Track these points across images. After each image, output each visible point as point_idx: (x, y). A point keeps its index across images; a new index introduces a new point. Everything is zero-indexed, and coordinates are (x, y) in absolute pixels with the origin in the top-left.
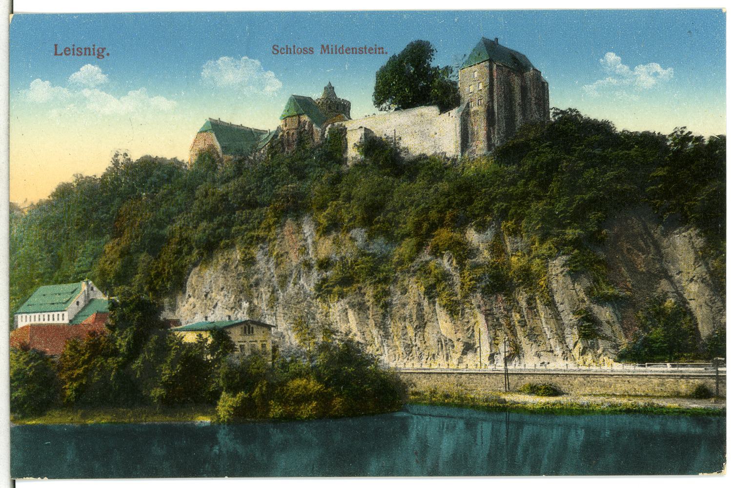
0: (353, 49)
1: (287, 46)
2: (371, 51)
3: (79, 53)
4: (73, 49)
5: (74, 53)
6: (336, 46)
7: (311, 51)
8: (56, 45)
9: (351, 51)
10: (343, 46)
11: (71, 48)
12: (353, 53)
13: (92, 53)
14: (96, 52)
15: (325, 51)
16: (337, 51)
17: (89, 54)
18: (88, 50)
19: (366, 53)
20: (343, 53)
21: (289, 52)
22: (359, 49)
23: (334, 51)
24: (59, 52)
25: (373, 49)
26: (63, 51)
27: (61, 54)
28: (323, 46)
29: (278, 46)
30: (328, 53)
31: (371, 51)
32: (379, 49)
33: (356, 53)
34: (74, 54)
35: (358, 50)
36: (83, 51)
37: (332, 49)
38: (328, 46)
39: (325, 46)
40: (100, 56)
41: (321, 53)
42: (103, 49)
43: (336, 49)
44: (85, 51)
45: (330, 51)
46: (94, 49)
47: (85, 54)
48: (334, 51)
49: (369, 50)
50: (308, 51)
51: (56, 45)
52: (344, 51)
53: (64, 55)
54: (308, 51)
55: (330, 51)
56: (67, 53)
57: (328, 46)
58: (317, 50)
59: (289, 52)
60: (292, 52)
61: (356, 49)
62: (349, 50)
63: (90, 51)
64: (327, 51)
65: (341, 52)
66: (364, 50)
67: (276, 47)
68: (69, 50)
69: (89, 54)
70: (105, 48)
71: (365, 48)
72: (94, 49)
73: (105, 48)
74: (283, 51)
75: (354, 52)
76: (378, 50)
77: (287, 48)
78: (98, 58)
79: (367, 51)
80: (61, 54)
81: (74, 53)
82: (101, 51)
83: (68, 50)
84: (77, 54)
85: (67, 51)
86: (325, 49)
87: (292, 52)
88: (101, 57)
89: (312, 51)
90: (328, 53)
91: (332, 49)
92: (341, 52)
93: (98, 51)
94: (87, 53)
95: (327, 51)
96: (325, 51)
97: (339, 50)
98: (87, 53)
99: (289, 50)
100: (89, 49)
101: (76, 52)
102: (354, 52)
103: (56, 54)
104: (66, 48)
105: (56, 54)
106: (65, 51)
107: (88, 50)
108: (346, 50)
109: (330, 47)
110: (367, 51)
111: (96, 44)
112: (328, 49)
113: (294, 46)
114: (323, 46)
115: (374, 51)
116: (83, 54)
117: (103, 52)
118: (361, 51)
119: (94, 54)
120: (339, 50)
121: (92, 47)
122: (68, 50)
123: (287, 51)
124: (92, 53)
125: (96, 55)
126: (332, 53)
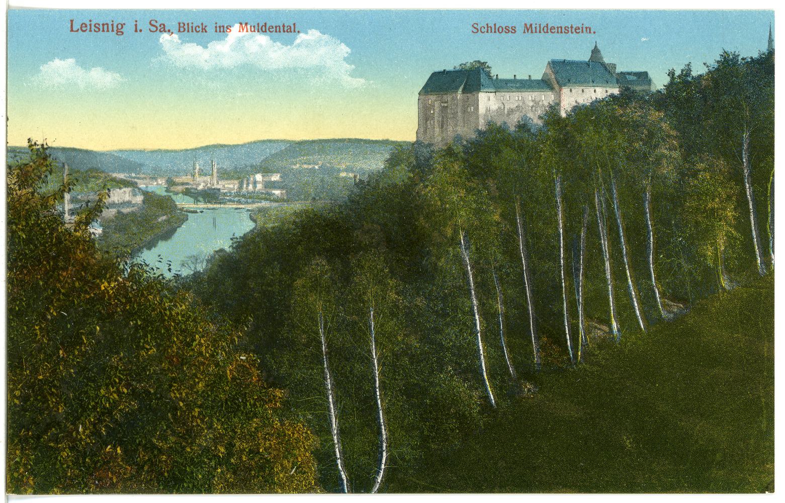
0: (558, 28)
2: (578, 31)
6: (540, 25)
7: (514, 30)
15: (528, 31)
16: (542, 30)
19: (572, 33)
20: (547, 32)
21: (489, 31)
22: (95, 26)
25: (579, 29)
28: (526, 25)
30: (532, 32)
31: (578, 31)
33: (561, 32)
35: (563, 30)
37: (536, 28)
38: (531, 25)
39: (528, 26)
41: (524, 32)
44: (103, 28)
45: (534, 30)
47: (103, 31)
49: (576, 29)
50: (510, 29)
52: (549, 31)
54: (510, 29)
55: (534, 30)
57: (531, 25)
58: (520, 29)
59: (489, 31)
60: (493, 31)
61: (561, 27)
64: (530, 31)
65: (545, 30)
66: (570, 30)
71: (572, 27)
76: (584, 30)
77: (488, 27)
79: (573, 30)
86: (528, 28)
87: (493, 31)
89: (514, 30)
90: (532, 32)
91: (536, 28)
92: (545, 29)
95: (530, 31)
96: (528, 31)
97: (543, 29)
108: (551, 29)
109: (533, 26)
110: (573, 30)
111: (194, 23)
112: (532, 29)
114: (526, 25)
115: (581, 30)
120: (543, 29)
123: (488, 30)
126: (536, 32)
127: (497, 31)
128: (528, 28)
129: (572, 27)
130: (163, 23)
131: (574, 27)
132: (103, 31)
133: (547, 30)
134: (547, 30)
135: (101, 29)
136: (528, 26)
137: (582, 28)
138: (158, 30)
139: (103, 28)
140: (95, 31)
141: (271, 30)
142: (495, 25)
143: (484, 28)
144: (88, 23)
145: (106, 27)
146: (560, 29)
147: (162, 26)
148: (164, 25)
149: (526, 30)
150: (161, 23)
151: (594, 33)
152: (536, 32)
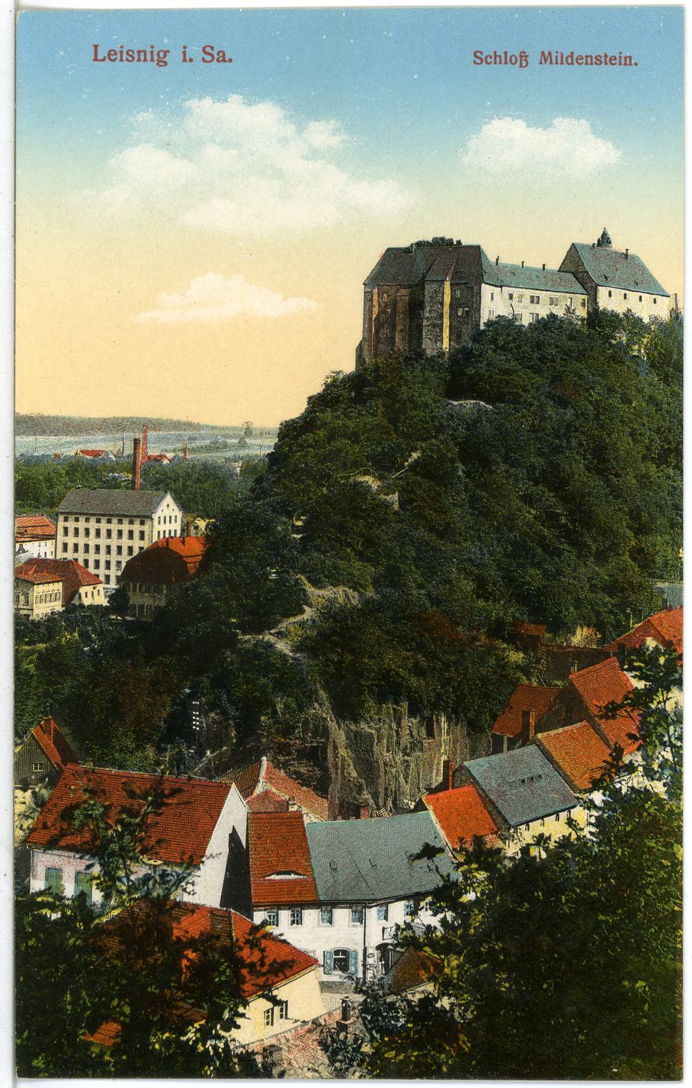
0: (587, 57)
1: (495, 53)
2: (614, 62)
3: (130, 59)
4: (121, 52)
5: (122, 56)
8: (96, 47)
9: (584, 61)
10: (572, 53)
12: (587, 64)
13: (149, 57)
14: (155, 57)
15: (546, 60)
17: (145, 60)
18: (142, 54)
19: (606, 64)
20: (572, 63)
23: (559, 61)
24: (100, 57)
25: (616, 59)
26: (106, 55)
27: (104, 60)
28: (543, 53)
29: (481, 53)
30: (551, 63)
31: (614, 62)
32: (625, 58)
33: (592, 64)
34: (121, 60)
35: (594, 60)
36: (136, 56)
37: (557, 57)
39: (546, 54)
40: (162, 62)
41: (541, 63)
42: (166, 53)
43: (562, 58)
44: (139, 55)
45: (554, 61)
46: (152, 52)
48: (559, 61)
49: (610, 60)
51: (96, 47)
52: (574, 62)
53: (107, 60)
55: (554, 61)
56: (113, 57)
57: (550, 54)
58: (534, 58)
60: (503, 61)
62: (582, 59)
63: (145, 55)
65: (570, 61)
66: (603, 60)
67: (478, 54)
68: (116, 54)
69: (145, 60)
70: (168, 51)
71: (606, 56)
72: (152, 52)
73: (168, 51)
74: (489, 60)
75: (589, 62)
76: (623, 60)
78: (158, 64)
79: (608, 60)
80: (104, 60)
81: (122, 56)
82: (162, 55)
83: (112, 53)
84: (127, 60)
85: (111, 56)
86: (546, 58)
87: (503, 61)
88: (161, 64)
90: (551, 63)
91: (557, 57)
92: (570, 61)
93: (158, 54)
94: (142, 58)
96: (546, 60)
98: (142, 58)
99: (498, 59)
100: (145, 52)
101: (125, 56)
102: (589, 62)
103: (96, 59)
104: (111, 51)
105: (96, 59)
106: (109, 54)
107: (142, 54)
108: (577, 59)
109: (554, 55)
110: (608, 60)
112: (551, 58)
113: (506, 53)
114: (543, 53)
115: (618, 61)
117: (165, 56)
118: (598, 60)
119: (152, 60)
120: (567, 63)
121: (149, 50)
122: (112, 53)
124: (149, 57)
125: (156, 62)
126: (557, 63)
127: (508, 61)
128: (546, 58)
129: (606, 56)
131: (609, 55)
132: (139, 60)
133: (572, 59)
134: (572, 59)
135: (603, 61)
136: (546, 54)
137: (620, 58)
141: (580, 61)
142: (506, 53)
143: (491, 58)
144: (617, 56)
145: (589, 59)
146: (589, 59)
149: (543, 61)
151: (636, 64)
152: (557, 63)
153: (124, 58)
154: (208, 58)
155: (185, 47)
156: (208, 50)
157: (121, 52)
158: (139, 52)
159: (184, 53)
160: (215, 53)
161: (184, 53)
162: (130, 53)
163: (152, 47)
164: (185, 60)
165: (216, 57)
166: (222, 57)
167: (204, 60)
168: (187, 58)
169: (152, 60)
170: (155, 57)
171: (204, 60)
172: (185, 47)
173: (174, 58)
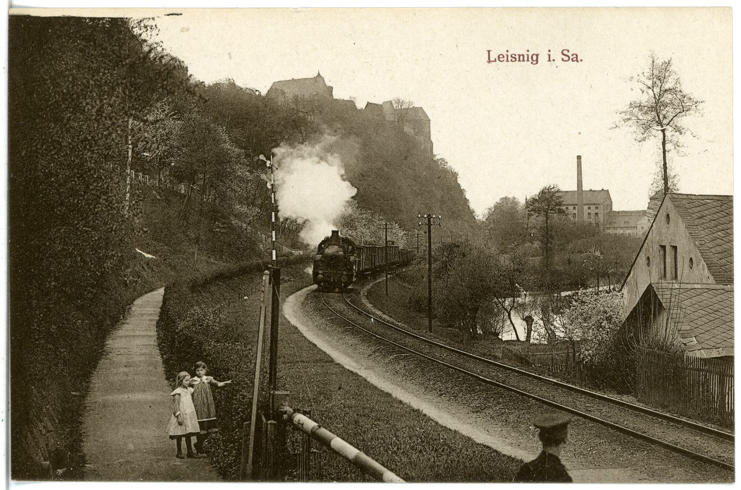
3: (514, 60)
5: (507, 59)
11: (505, 54)
13: (526, 58)
14: (530, 59)
17: (524, 60)
36: (517, 57)
44: (519, 58)
47: (519, 61)
68: (504, 57)
78: (532, 63)
80: (495, 61)
81: (507, 59)
101: (510, 58)
104: (501, 55)
106: (499, 57)
116: (518, 59)
119: (528, 60)
124: (526, 58)
130: (576, 53)
132: (519, 61)
138: (571, 59)
139: (519, 58)
140: (511, 60)
147: (575, 56)
148: (577, 55)
150: (512, 53)
153: (509, 60)
154: (566, 58)
155: (549, 51)
156: (565, 52)
157: (507, 55)
158: (519, 56)
159: (549, 55)
160: (570, 54)
161: (549, 55)
162: (513, 56)
163: (528, 51)
164: (549, 60)
165: (571, 57)
166: (576, 58)
167: (563, 60)
168: (551, 59)
169: (528, 60)
170: (530, 59)
171: (563, 60)
172: (549, 51)
173: (543, 58)
